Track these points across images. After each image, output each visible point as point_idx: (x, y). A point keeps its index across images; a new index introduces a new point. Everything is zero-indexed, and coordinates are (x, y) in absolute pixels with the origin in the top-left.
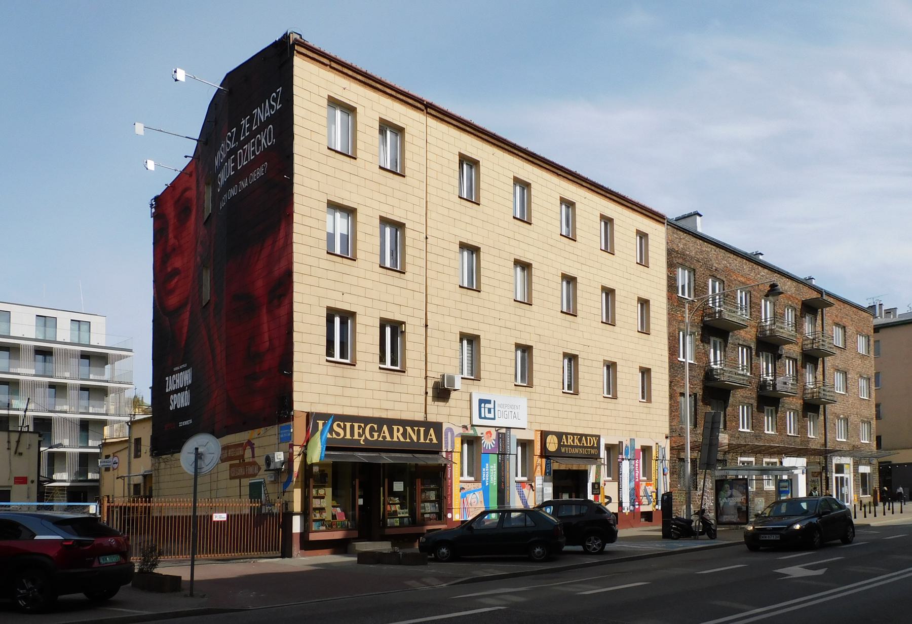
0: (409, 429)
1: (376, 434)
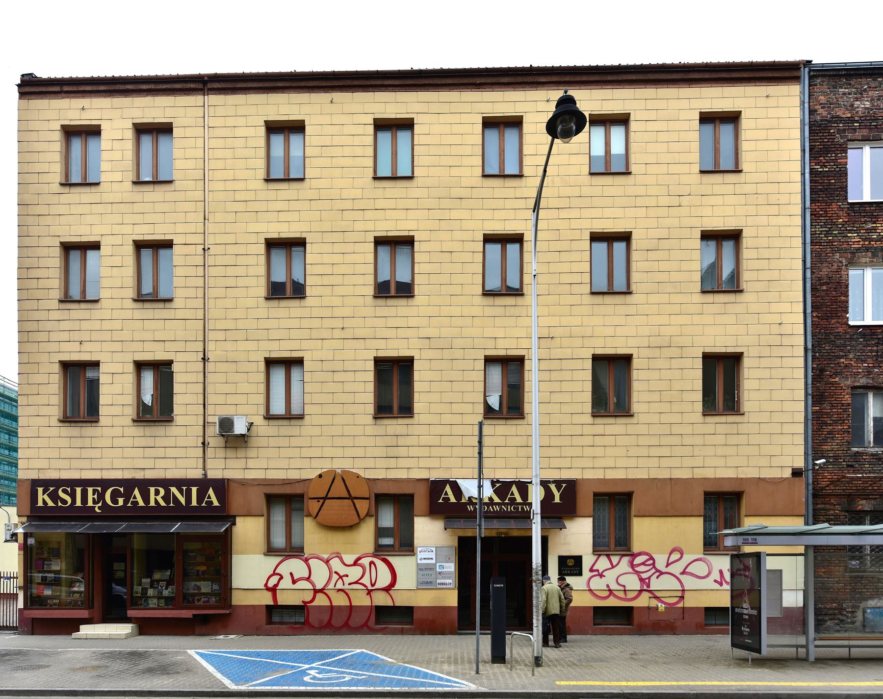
0: (174, 490)
1: (121, 501)
